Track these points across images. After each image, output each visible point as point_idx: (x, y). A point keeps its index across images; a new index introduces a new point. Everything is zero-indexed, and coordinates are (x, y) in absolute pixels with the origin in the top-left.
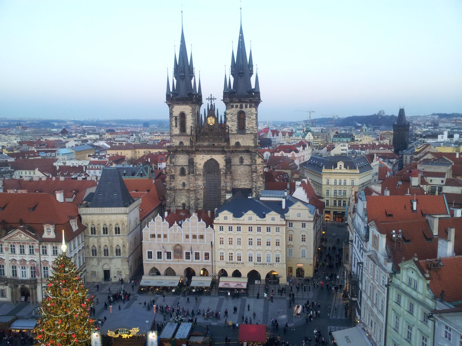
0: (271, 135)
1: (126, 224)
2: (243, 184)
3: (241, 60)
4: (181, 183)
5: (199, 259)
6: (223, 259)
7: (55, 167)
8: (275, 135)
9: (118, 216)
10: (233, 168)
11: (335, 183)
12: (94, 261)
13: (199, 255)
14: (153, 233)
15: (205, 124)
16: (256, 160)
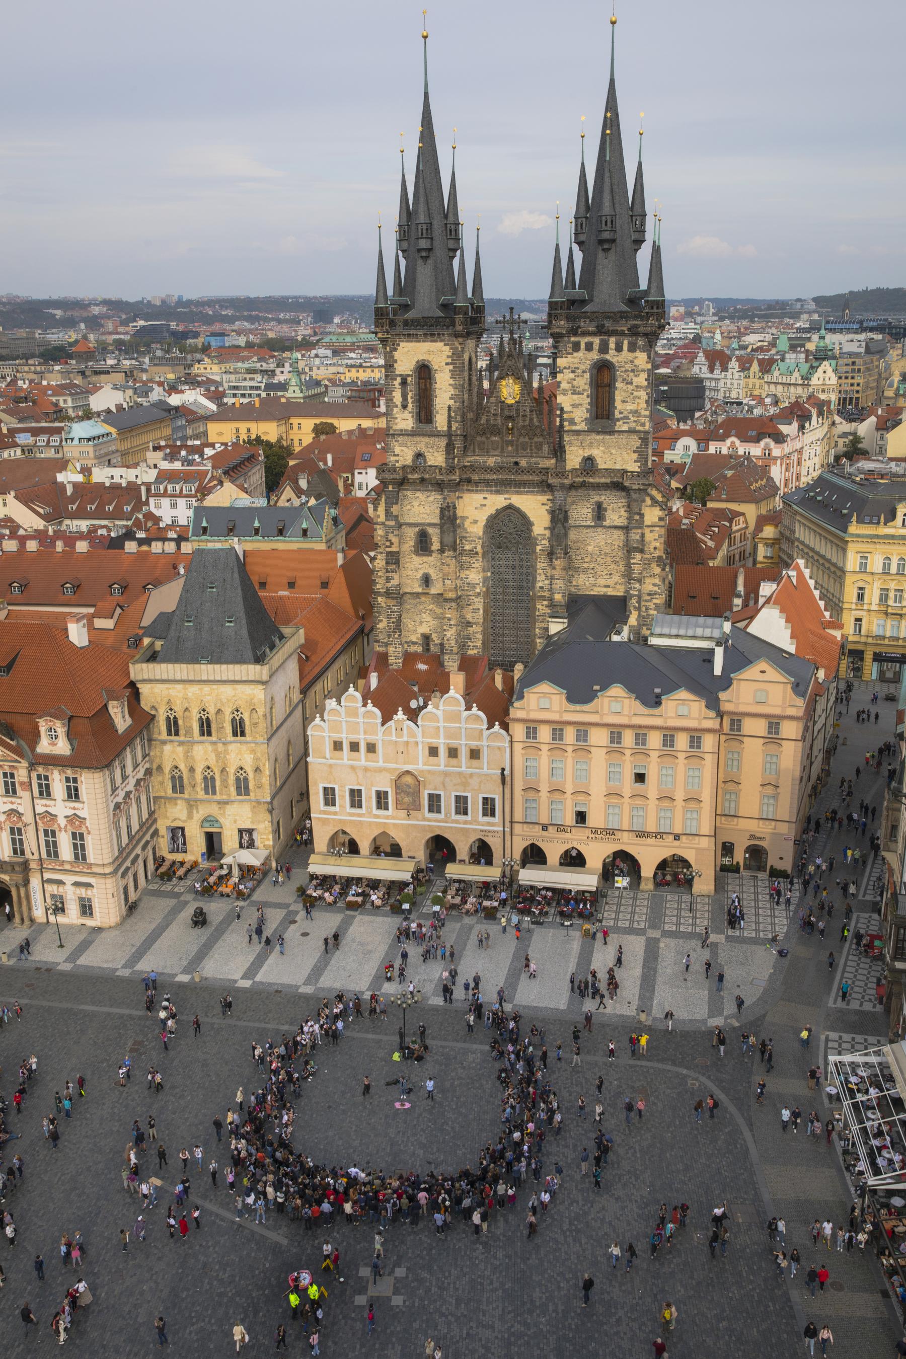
0: (705, 369)
1: (261, 711)
2: (602, 582)
3: (607, 197)
4: (419, 575)
5: (465, 813)
7: (62, 486)
8: (718, 364)
9: (239, 687)
10: (573, 535)
11: (887, 566)
12: (179, 807)
13: (466, 802)
14: (336, 736)
15: (493, 400)
16: (642, 515)
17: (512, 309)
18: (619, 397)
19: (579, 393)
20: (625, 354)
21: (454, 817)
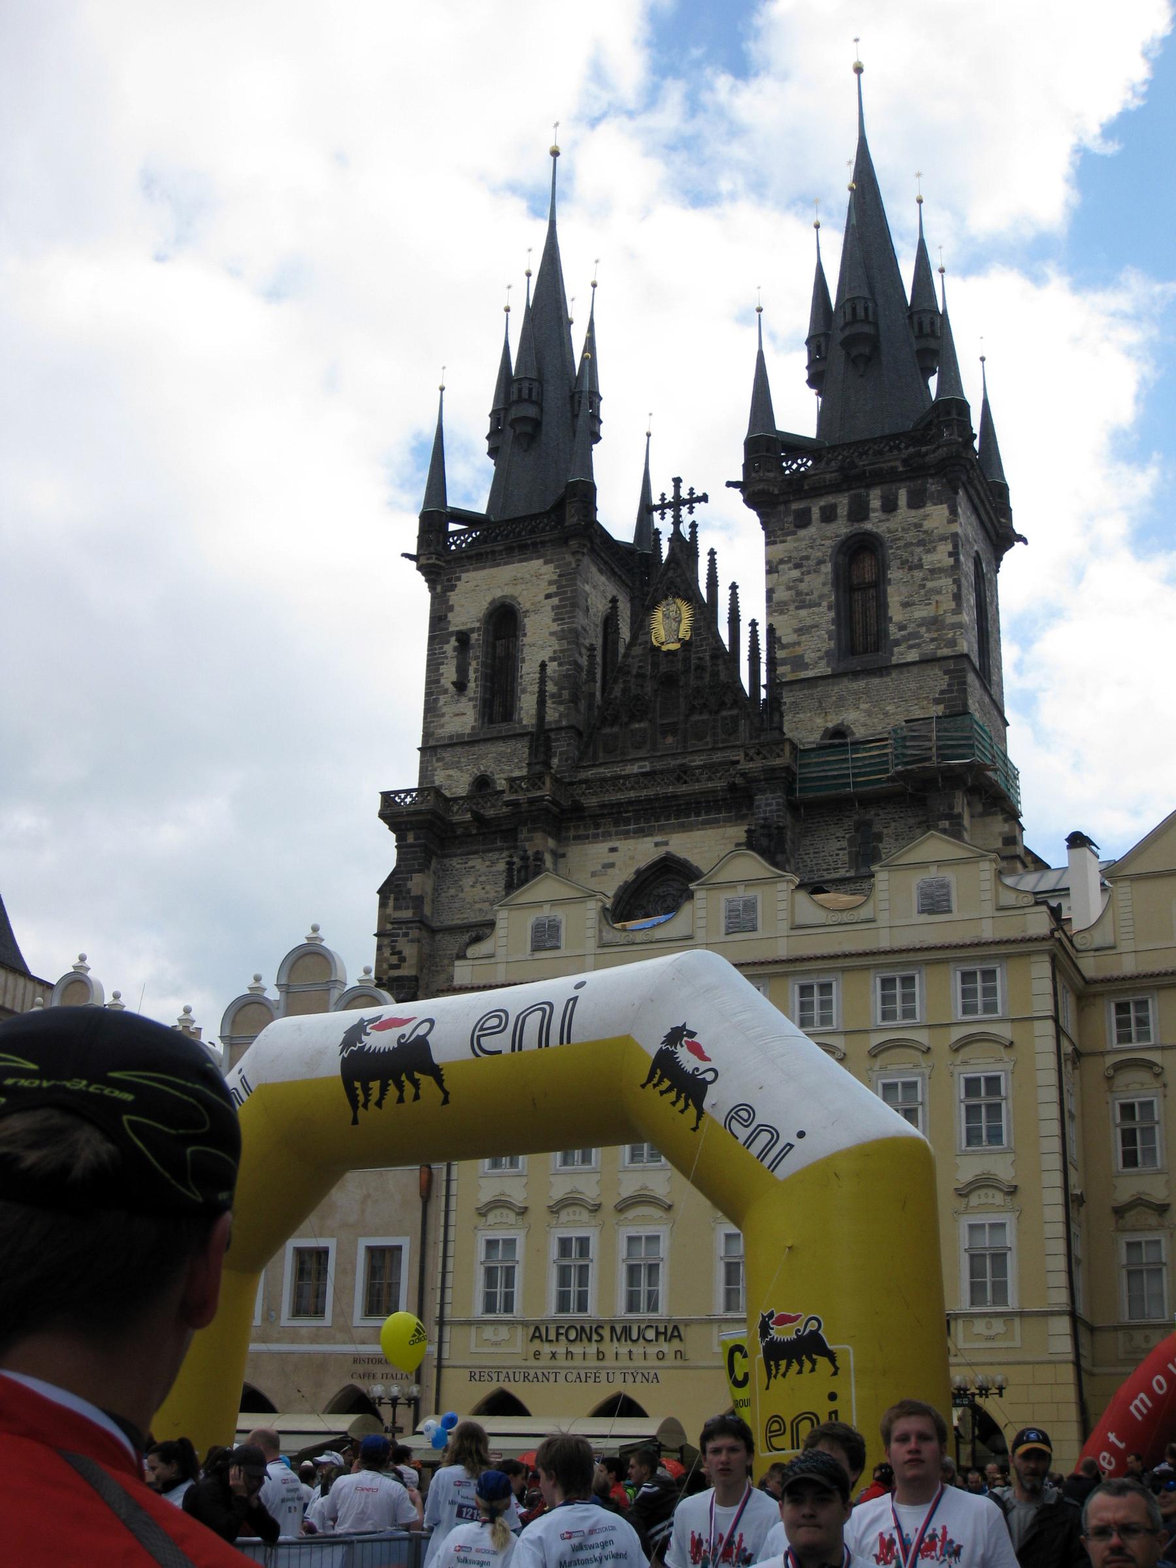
6: (508, 1308)
15: (637, 650)
17: (677, 481)
18: (894, 597)
19: (810, 606)
20: (904, 513)
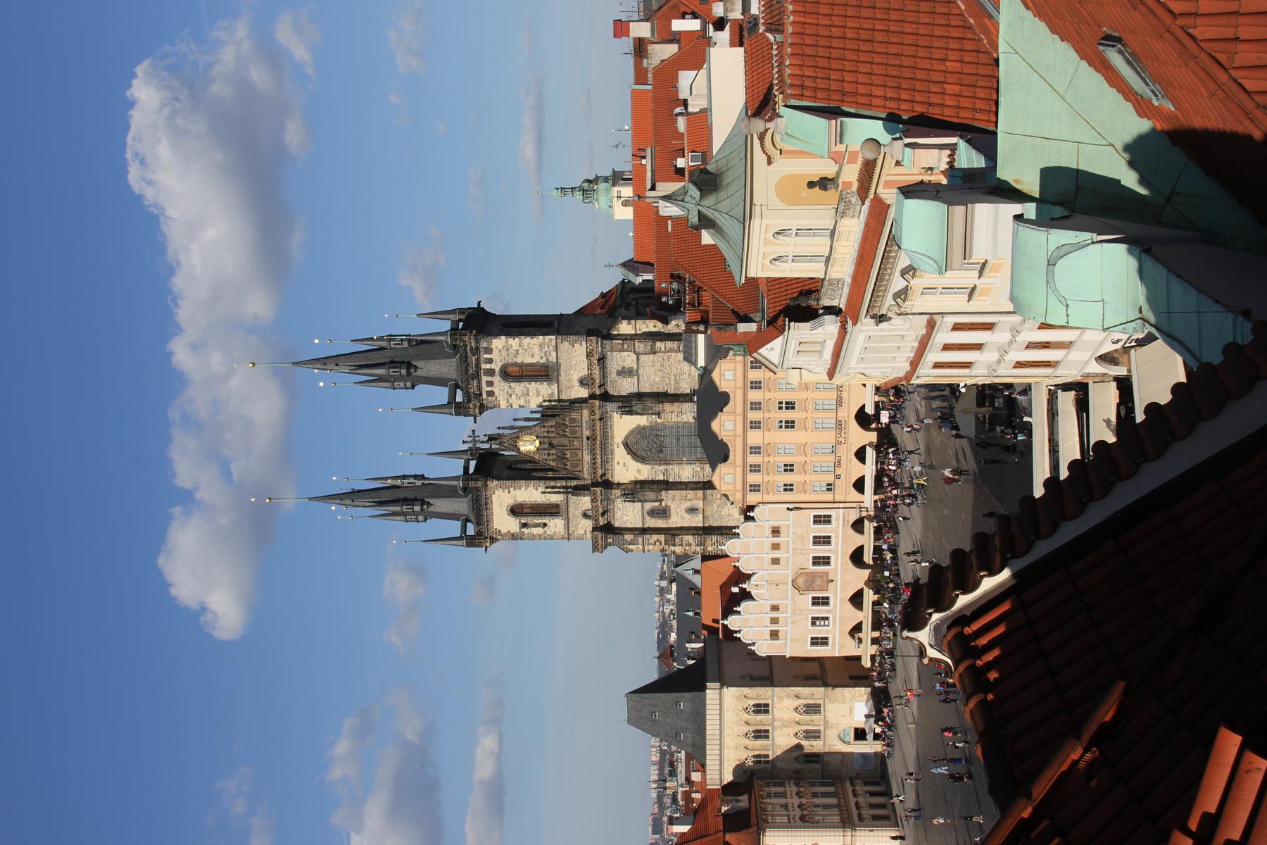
1: (745, 690)
4: (687, 516)
9: (726, 705)
14: (767, 636)
18: (529, 360)
21: (832, 547)
